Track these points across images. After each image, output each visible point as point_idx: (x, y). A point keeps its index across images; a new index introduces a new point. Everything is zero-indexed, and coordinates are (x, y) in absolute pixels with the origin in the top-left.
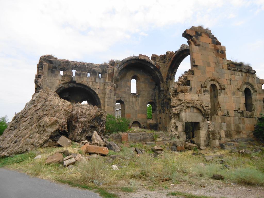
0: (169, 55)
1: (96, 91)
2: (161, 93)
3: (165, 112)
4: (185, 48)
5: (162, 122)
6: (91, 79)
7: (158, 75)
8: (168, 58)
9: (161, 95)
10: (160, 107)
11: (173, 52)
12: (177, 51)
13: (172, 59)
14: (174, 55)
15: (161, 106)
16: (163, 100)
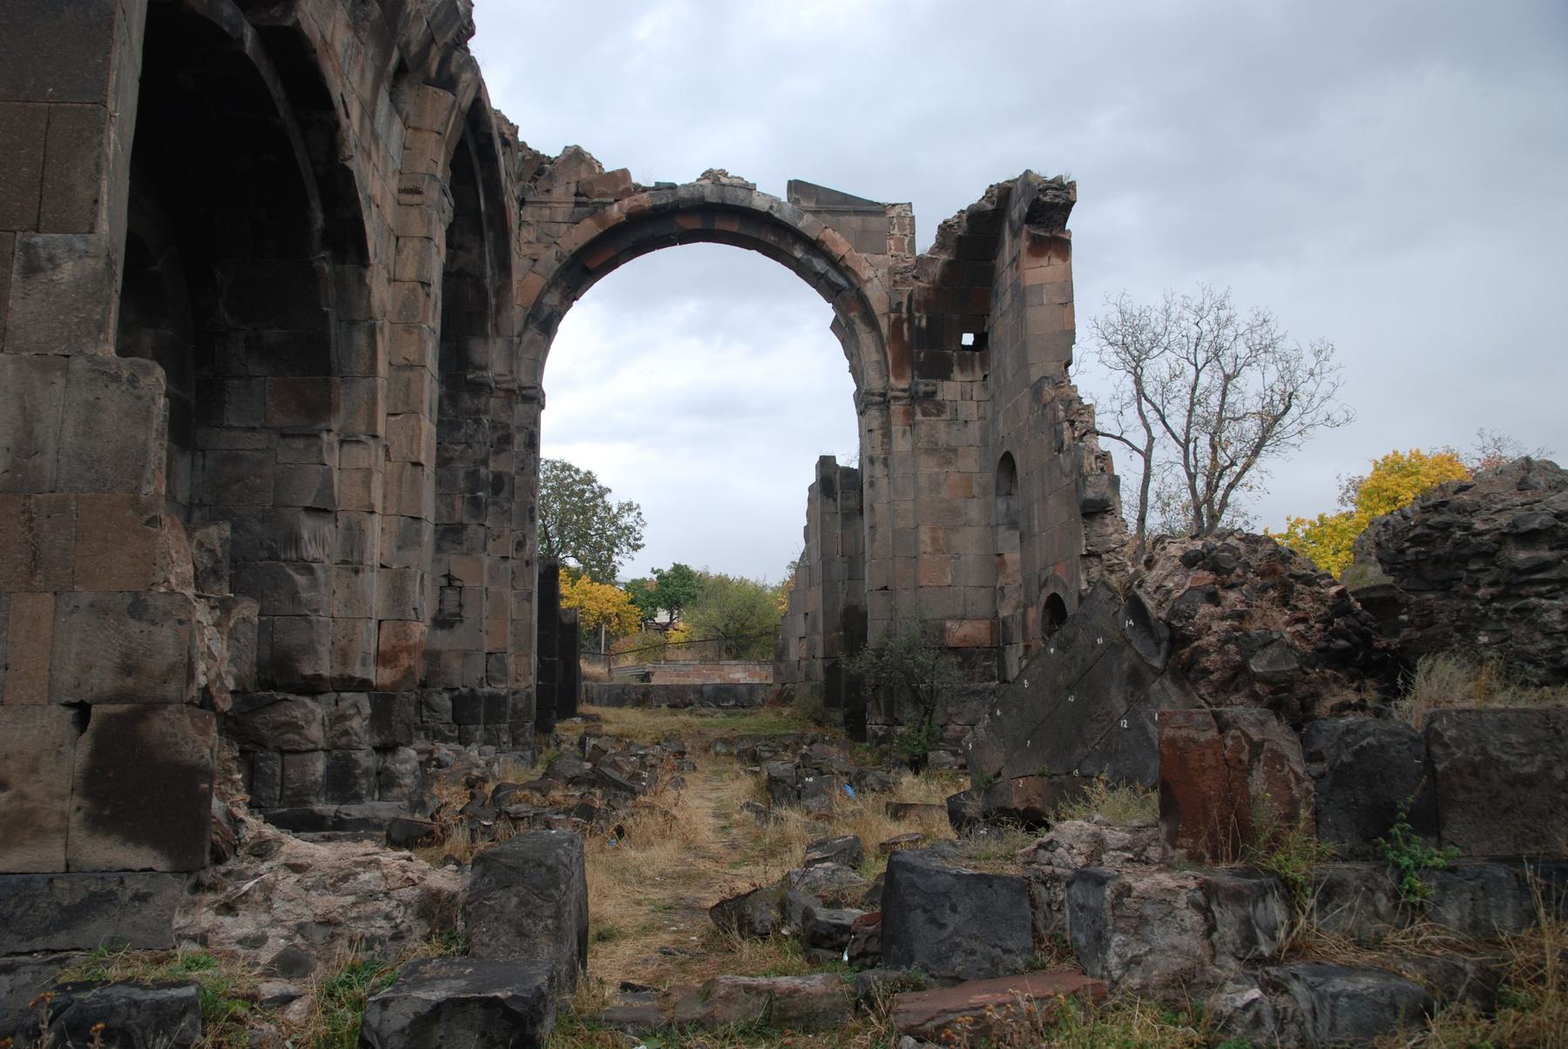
0: (584, 175)
1: (370, 227)
2: (467, 400)
3: (491, 545)
4: (759, 204)
5: (468, 614)
6: (363, 71)
7: (489, 271)
8: (573, 189)
9: (478, 422)
10: (459, 504)
11: (625, 173)
12: (672, 187)
13: (616, 212)
14: (645, 200)
15: (476, 505)
16: (485, 462)
